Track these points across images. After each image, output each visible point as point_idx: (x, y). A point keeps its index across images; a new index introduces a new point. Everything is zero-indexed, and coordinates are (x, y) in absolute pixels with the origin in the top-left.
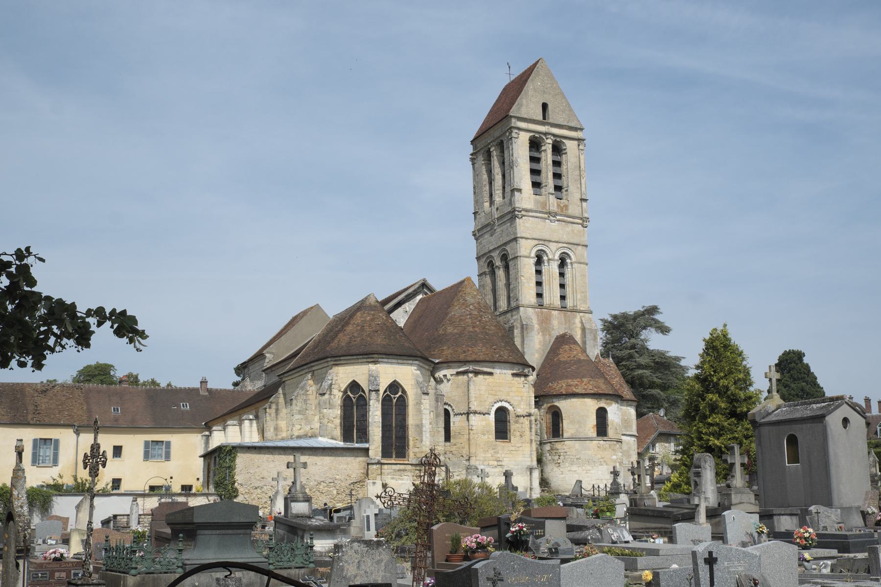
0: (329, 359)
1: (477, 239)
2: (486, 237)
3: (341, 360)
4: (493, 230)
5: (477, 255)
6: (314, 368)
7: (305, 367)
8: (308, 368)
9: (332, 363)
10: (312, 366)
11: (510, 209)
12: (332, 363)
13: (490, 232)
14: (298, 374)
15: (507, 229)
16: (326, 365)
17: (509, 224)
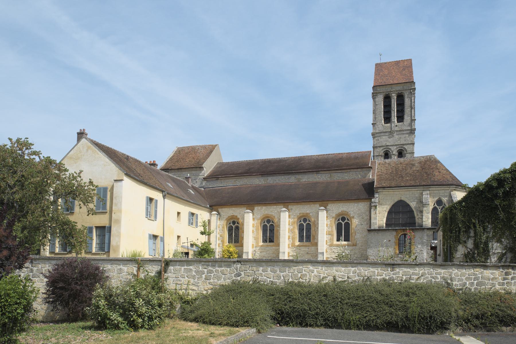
0: (454, 186)
1: (374, 138)
2: (384, 138)
3: (457, 188)
4: (391, 136)
5: (374, 145)
6: (430, 189)
7: (422, 187)
8: (423, 188)
9: (454, 189)
10: (430, 188)
11: (409, 128)
12: (454, 189)
13: (388, 136)
14: (406, 190)
15: (405, 137)
16: (448, 188)
17: (408, 135)
